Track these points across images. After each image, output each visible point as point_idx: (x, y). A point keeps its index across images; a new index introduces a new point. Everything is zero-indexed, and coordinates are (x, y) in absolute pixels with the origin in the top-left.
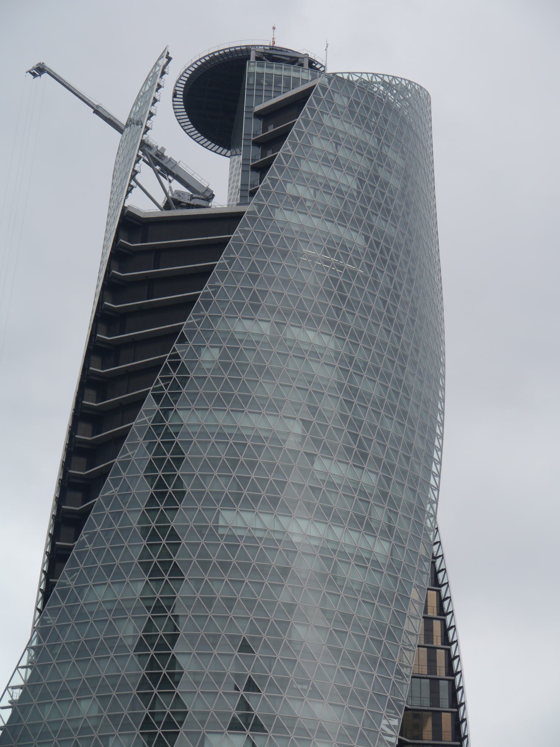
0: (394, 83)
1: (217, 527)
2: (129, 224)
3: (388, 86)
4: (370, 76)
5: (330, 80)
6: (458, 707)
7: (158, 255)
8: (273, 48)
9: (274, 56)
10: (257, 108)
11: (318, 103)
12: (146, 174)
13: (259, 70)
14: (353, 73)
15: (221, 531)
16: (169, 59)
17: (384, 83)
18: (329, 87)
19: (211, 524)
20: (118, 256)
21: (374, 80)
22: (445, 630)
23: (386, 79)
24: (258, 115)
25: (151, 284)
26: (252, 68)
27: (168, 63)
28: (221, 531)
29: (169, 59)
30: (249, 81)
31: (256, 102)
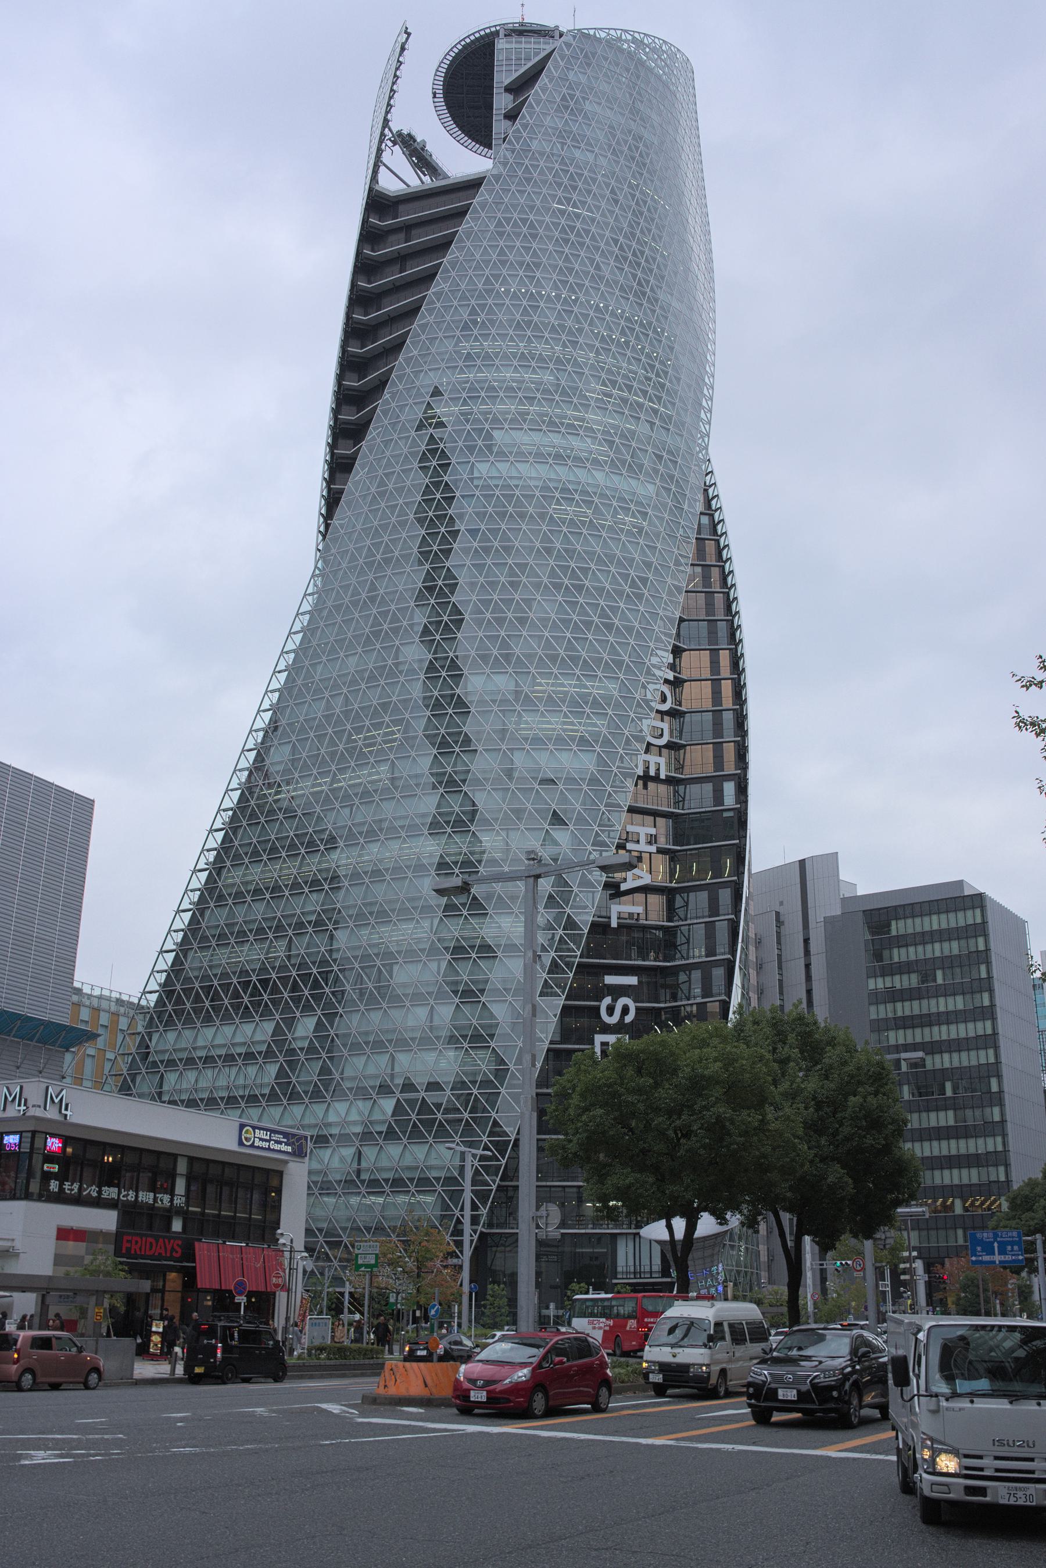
0: (646, 41)
1: (471, 480)
2: (378, 203)
3: (639, 43)
4: (619, 32)
5: (574, 37)
6: (737, 645)
7: (408, 228)
8: (522, 24)
9: (522, 31)
10: (507, 82)
11: (562, 60)
12: (396, 158)
13: (508, 46)
14: (601, 29)
15: (476, 482)
16: (409, 34)
17: (634, 40)
18: (574, 44)
19: (465, 476)
20: (368, 236)
21: (624, 37)
22: (724, 577)
23: (636, 35)
24: (508, 89)
25: (402, 259)
26: (501, 44)
27: (407, 39)
28: (476, 482)
29: (409, 34)
30: (499, 57)
31: (503, 76)
